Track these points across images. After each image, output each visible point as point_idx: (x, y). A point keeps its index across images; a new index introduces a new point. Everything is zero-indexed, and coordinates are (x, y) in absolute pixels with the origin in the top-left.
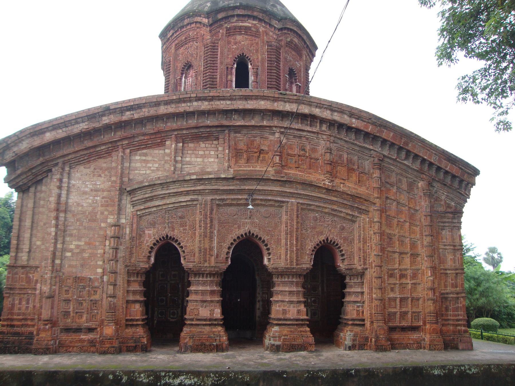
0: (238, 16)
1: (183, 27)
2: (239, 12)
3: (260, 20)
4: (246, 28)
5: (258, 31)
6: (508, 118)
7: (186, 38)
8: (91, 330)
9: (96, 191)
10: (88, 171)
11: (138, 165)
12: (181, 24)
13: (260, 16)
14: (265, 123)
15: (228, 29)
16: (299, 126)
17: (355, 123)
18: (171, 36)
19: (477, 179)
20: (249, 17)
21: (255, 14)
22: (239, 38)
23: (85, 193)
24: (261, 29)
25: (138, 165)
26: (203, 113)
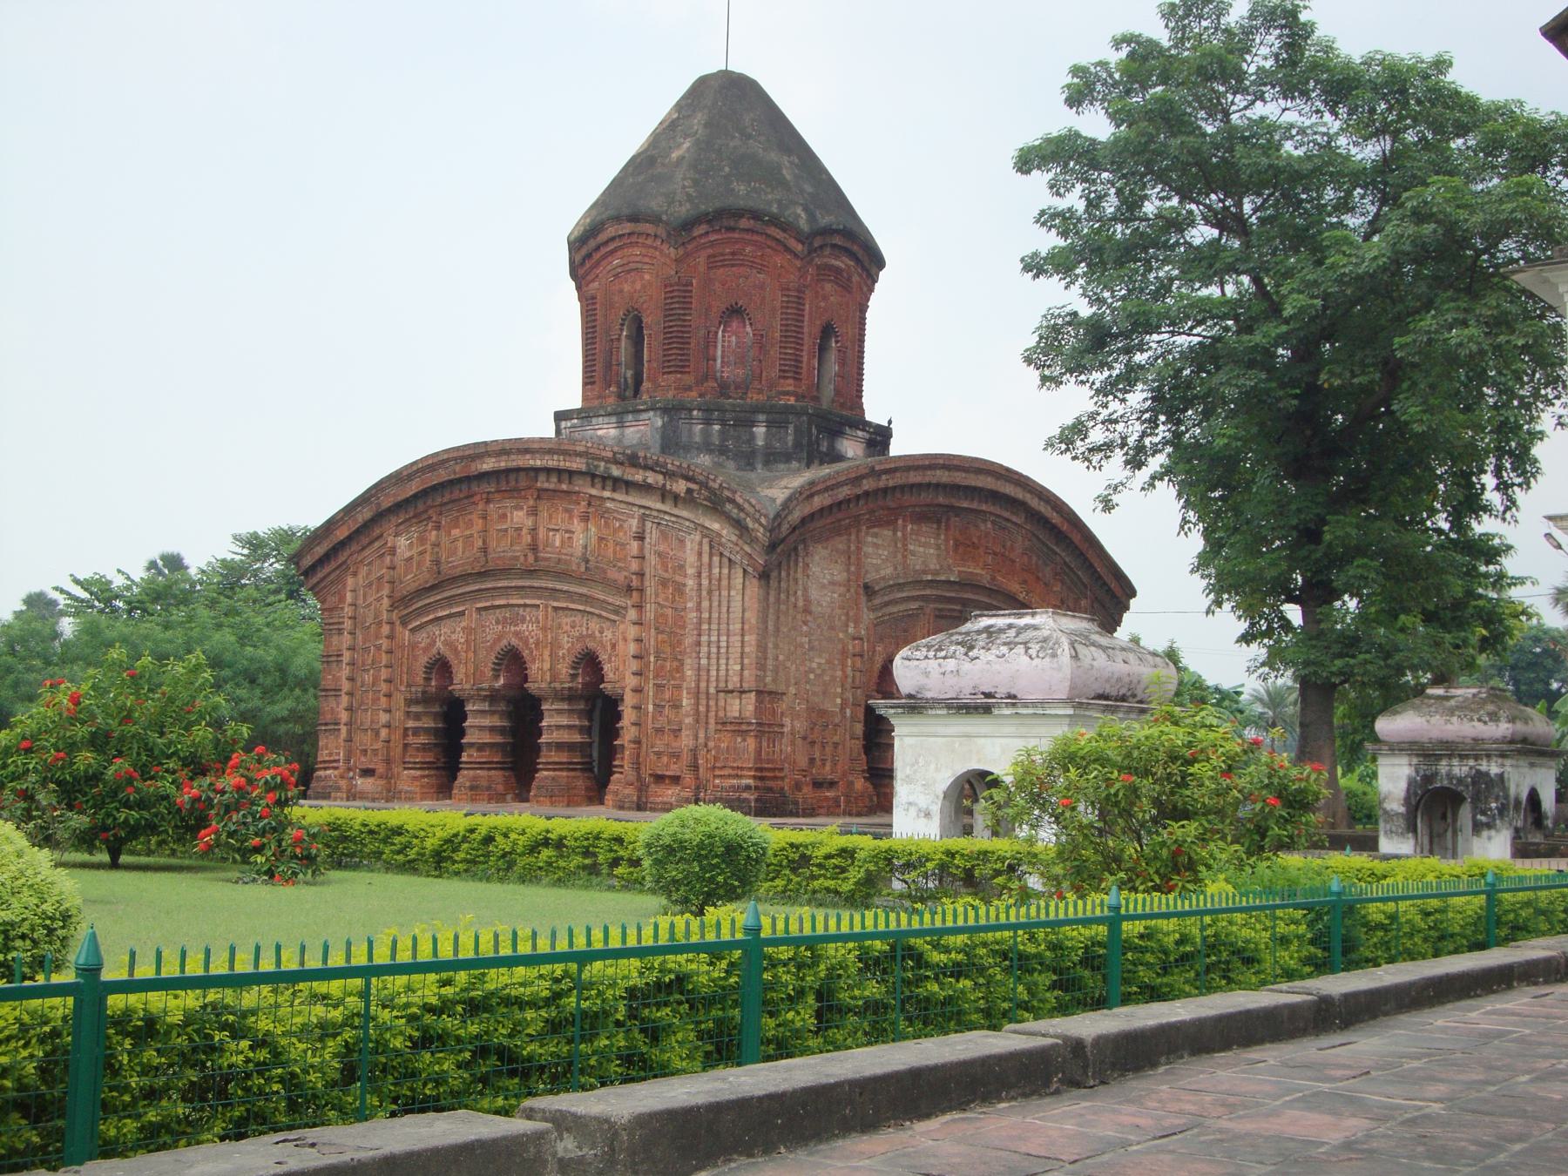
0: (834, 246)
1: (731, 229)
2: (837, 240)
3: (857, 260)
4: (838, 271)
5: (849, 279)
6: (1115, 498)
7: (733, 254)
8: (832, 784)
9: (832, 583)
10: (825, 553)
11: (870, 550)
12: (732, 223)
13: (860, 254)
14: (984, 507)
15: (818, 267)
16: (1006, 514)
17: (1056, 519)
18: (701, 236)
19: (1132, 601)
20: (847, 251)
21: (855, 248)
22: (828, 286)
23: (823, 586)
24: (856, 278)
25: (870, 550)
26: (938, 486)
